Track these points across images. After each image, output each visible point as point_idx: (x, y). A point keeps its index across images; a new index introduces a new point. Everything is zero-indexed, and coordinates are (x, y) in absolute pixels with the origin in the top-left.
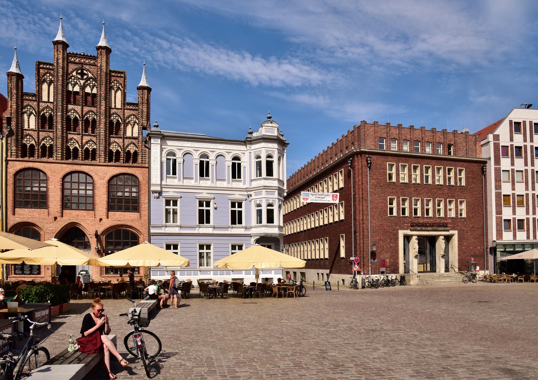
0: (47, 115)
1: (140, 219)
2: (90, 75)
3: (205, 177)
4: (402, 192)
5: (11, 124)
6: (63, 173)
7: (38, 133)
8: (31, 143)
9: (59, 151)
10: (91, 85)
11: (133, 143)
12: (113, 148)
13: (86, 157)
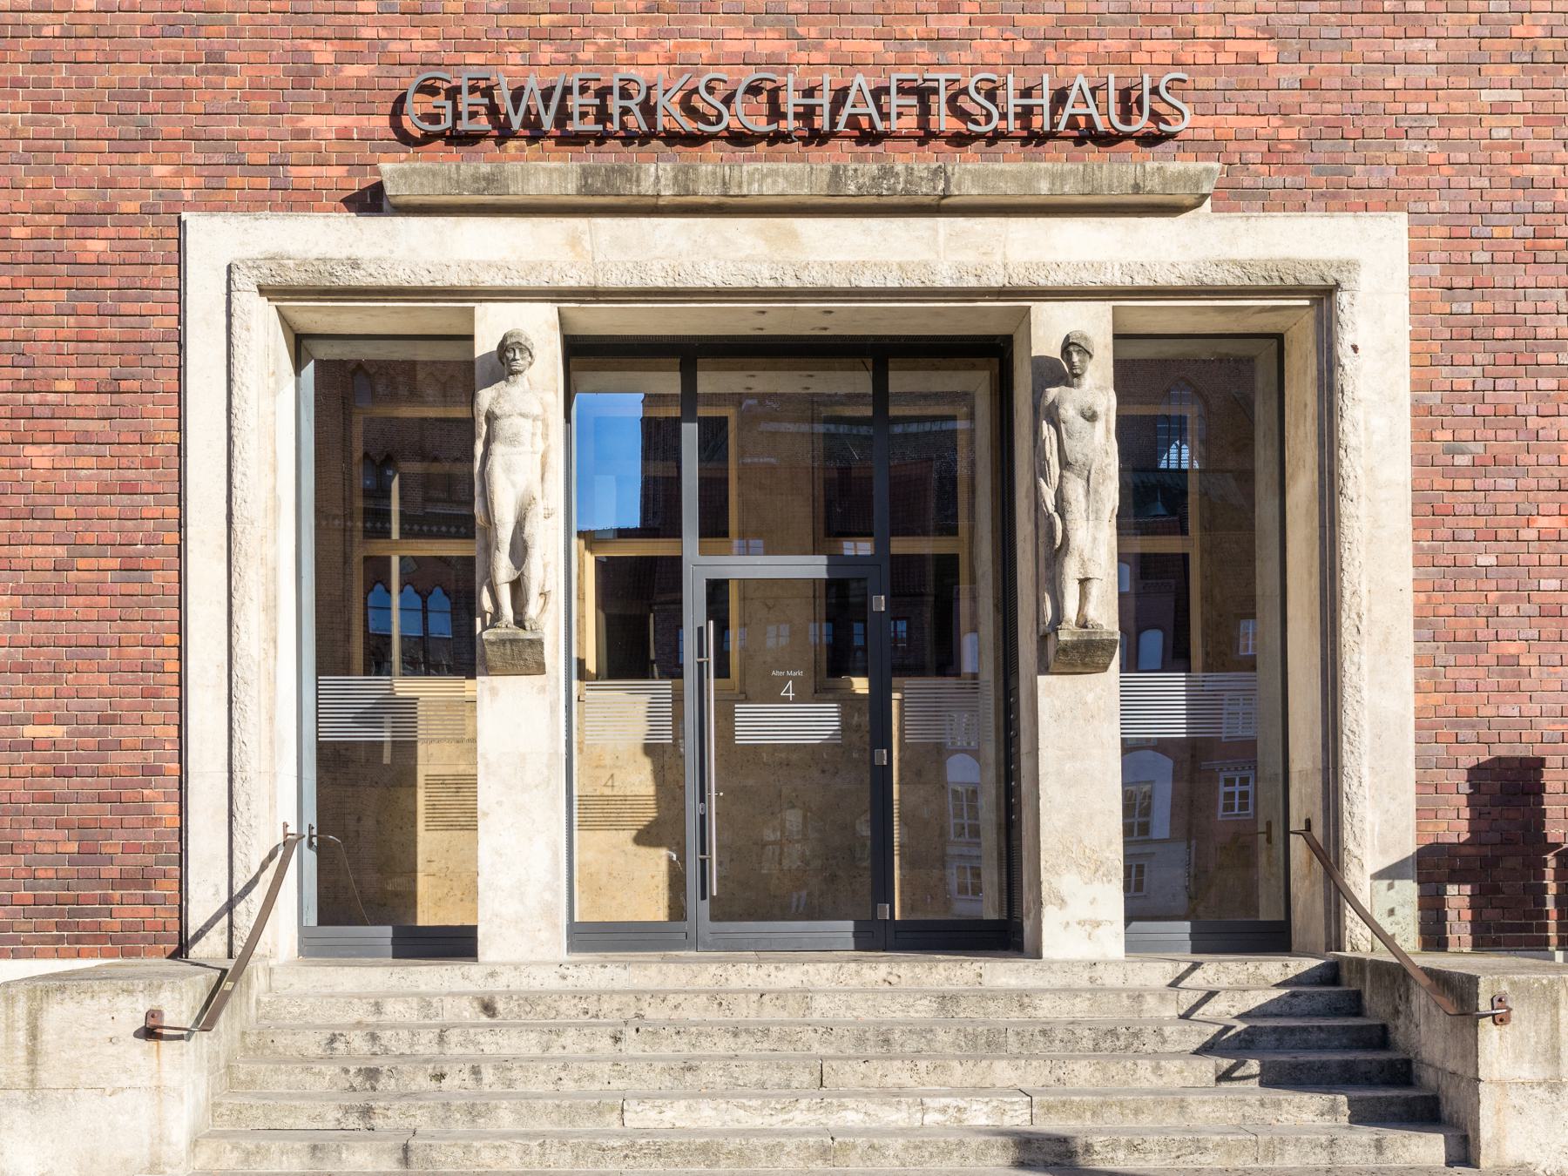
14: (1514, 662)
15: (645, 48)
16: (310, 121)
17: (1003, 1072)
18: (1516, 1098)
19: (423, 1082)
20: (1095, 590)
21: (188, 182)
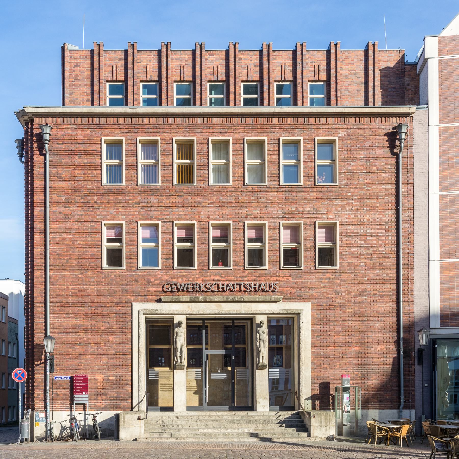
4: (143, 207)
14: (326, 368)
15: (199, 278)
16: (150, 289)
17: (250, 426)
18: (316, 428)
19: (171, 427)
20: (264, 358)
21: (132, 298)
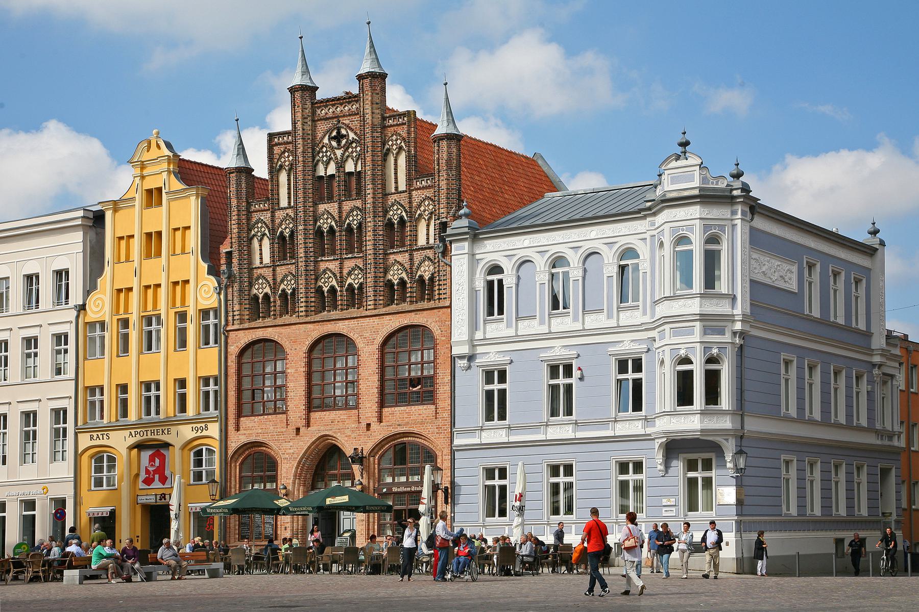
0: (287, 233)
1: (436, 418)
2: (352, 135)
3: (561, 309)
5: (232, 263)
6: (309, 342)
7: (274, 270)
8: (265, 291)
9: (302, 300)
10: (354, 154)
11: (428, 257)
12: (393, 275)
13: (351, 304)
